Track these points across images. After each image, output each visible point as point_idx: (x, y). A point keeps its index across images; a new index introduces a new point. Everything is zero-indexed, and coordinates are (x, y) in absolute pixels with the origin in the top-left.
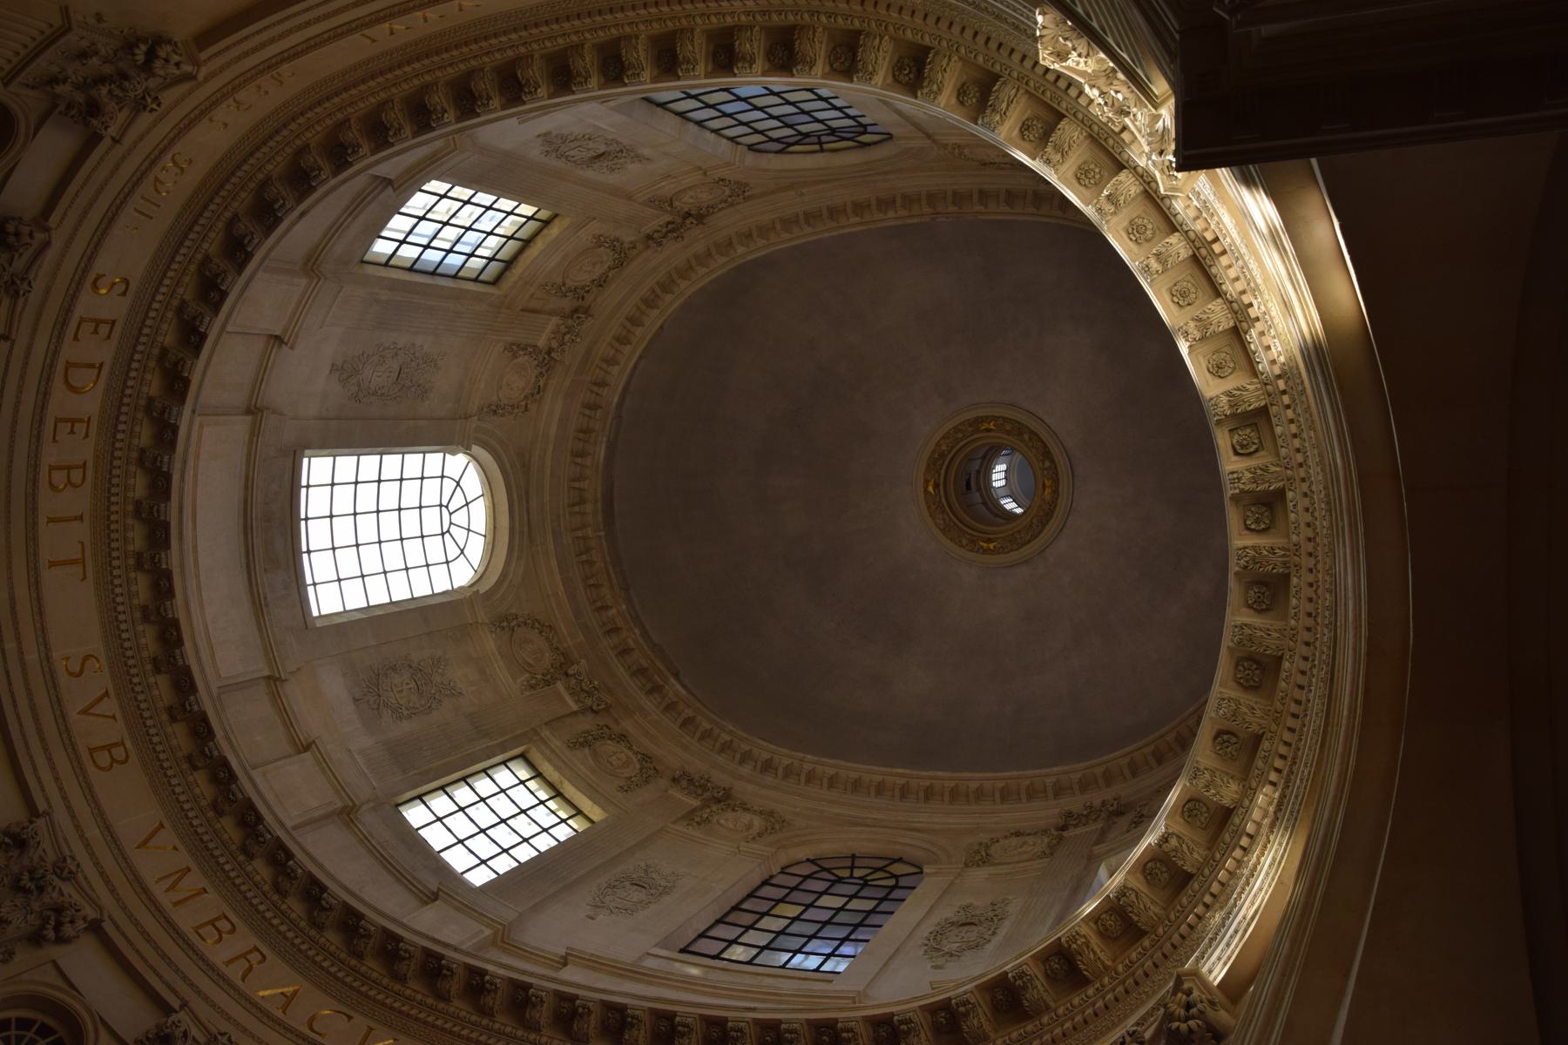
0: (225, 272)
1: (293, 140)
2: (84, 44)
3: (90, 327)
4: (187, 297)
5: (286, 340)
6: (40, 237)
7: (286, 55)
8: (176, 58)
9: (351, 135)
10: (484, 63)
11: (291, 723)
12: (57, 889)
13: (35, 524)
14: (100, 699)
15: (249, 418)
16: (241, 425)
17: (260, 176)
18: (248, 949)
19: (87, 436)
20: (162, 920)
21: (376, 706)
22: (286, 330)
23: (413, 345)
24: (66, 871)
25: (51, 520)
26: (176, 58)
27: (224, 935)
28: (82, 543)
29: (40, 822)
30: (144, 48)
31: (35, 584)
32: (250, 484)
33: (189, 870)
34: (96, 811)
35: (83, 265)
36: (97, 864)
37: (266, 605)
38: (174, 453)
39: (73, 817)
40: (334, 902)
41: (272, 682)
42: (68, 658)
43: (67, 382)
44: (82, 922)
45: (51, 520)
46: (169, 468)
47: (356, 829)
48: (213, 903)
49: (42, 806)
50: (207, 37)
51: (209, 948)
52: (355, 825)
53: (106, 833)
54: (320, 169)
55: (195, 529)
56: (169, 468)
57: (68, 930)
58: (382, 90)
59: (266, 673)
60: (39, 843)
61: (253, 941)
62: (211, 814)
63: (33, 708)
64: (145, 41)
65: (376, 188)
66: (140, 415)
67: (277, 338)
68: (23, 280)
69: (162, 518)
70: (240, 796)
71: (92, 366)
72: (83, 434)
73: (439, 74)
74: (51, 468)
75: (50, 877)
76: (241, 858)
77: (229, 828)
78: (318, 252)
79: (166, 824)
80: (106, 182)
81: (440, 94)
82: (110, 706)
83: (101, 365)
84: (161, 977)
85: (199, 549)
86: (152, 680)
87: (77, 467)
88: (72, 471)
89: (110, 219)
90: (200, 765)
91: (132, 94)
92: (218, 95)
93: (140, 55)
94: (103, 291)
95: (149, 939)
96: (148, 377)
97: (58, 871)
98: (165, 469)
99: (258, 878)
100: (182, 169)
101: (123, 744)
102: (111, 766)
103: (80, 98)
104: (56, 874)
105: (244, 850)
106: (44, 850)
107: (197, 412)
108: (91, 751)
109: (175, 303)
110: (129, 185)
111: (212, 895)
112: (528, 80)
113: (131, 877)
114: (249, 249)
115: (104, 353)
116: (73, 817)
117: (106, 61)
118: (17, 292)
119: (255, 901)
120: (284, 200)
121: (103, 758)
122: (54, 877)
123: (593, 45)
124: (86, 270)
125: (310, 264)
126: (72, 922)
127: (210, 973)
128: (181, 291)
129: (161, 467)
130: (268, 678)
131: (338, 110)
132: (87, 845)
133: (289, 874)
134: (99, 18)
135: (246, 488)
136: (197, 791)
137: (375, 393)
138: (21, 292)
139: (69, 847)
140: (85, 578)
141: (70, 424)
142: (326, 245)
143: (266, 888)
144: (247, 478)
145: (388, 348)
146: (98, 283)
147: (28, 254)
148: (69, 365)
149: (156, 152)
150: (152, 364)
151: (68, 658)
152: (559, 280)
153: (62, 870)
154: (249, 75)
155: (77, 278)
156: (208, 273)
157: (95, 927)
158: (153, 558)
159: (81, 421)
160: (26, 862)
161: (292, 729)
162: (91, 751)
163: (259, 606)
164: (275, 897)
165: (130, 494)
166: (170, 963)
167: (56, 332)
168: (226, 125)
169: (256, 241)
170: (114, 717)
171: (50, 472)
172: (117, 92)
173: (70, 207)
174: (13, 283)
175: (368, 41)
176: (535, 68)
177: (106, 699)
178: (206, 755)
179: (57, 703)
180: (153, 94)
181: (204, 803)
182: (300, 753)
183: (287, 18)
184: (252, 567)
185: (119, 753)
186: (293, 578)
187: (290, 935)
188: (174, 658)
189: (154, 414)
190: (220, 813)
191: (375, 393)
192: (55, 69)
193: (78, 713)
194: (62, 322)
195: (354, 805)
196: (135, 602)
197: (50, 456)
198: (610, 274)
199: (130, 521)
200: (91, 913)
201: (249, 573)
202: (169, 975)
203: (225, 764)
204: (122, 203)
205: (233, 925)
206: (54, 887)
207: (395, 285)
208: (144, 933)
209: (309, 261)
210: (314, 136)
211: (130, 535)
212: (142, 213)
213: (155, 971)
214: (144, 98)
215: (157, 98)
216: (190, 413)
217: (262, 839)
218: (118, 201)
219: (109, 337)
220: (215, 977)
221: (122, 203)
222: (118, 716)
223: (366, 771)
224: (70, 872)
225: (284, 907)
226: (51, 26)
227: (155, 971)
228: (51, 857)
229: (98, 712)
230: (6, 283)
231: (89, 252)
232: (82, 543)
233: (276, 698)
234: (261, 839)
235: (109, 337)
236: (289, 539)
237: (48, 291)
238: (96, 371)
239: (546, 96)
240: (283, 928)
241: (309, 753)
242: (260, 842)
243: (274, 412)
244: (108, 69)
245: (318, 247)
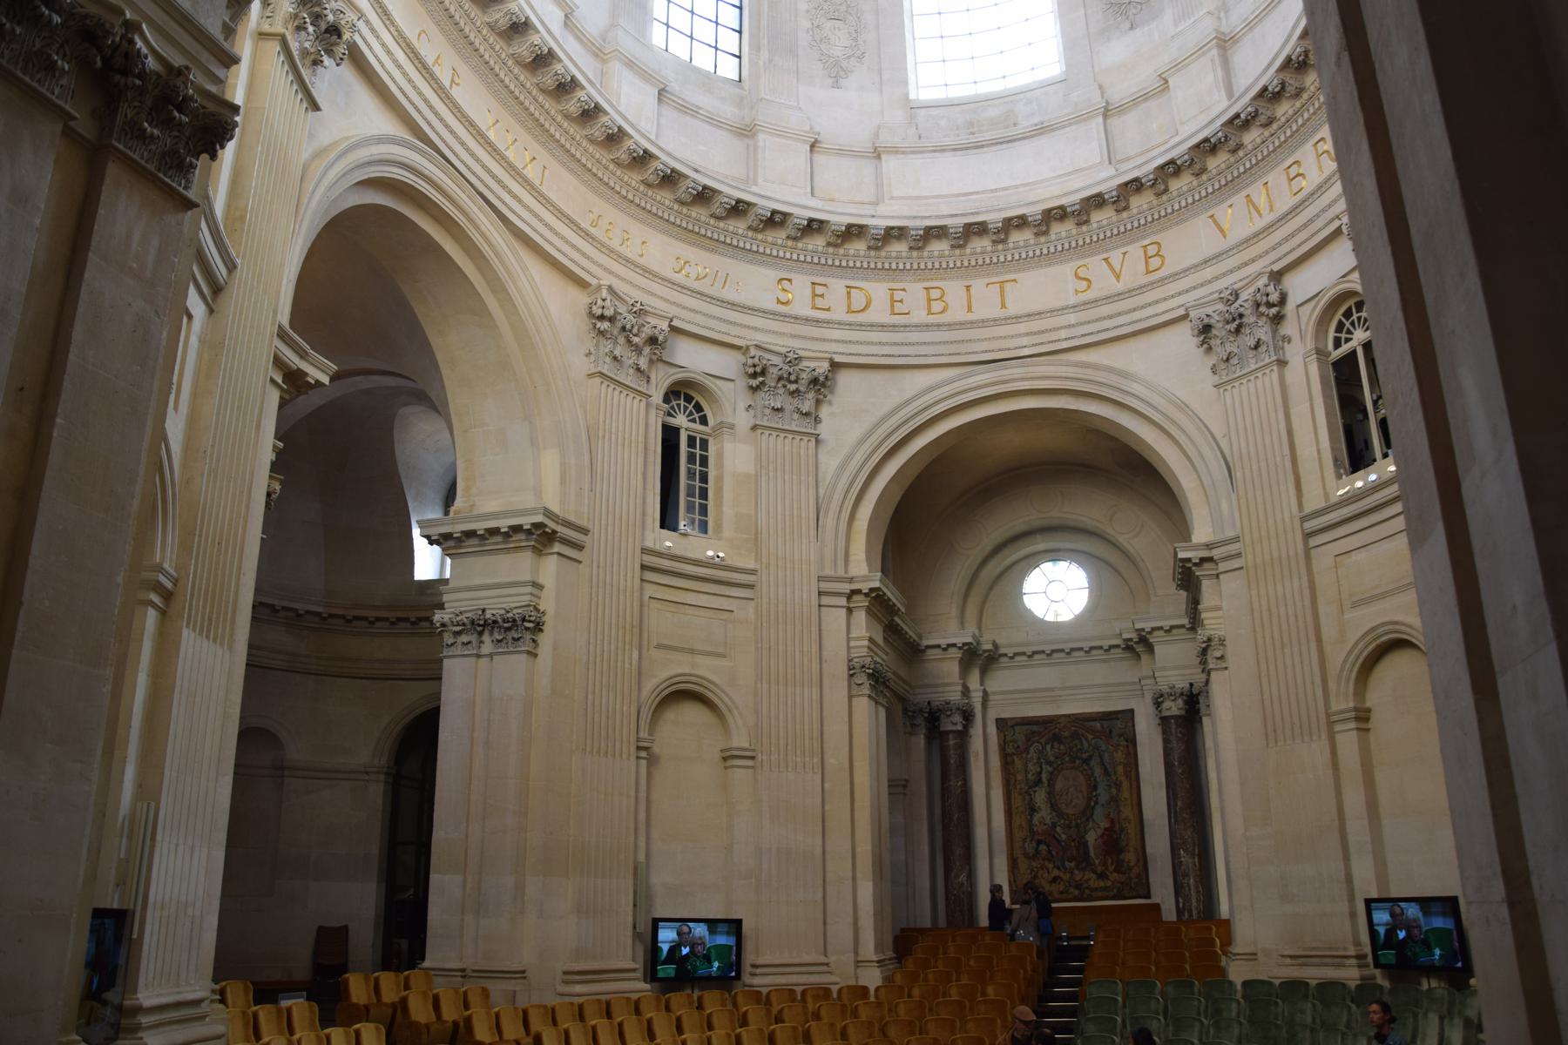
0: (756, 216)
1: (641, 192)
2: (608, 360)
3: (818, 300)
4: (784, 236)
5: (813, 140)
6: (753, 352)
7: (575, 228)
8: (600, 302)
9: (622, 156)
10: (532, 85)
11: (1145, 94)
12: (1242, 304)
13: (971, 322)
14: (1109, 264)
15: (884, 157)
16: (890, 163)
17: (676, 207)
18: (1314, 152)
19: (904, 290)
20: (1280, 224)
21: (1139, 7)
22: (805, 142)
23: (808, 11)
24: (1230, 297)
25: (970, 309)
26: (600, 302)
27: (1301, 172)
28: (988, 284)
29: (1192, 314)
30: (599, 324)
31: (1017, 319)
32: (939, 148)
33: (1248, 196)
34: (1192, 271)
35: (771, 316)
36: (1231, 271)
37: (1042, 124)
38: (907, 227)
39: (1194, 288)
40: (1275, 81)
41: (1109, 113)
42: (1076, 290)
43: (859, 312)
44: (1269, 288)
45: (970, 309)
46: (921, 229)
47: (1240, 34)
48: (1276, 177)
49: (1181, 312)
50: (582, 284)
51: (1307, 185)
52: (1236, 34)
53: (1209, 263)
54: (656, 170)
55: (977, 193)
56: (921, 229)
57: (1274, 297)
58: (581, 146)
59: (1100, 119)
60: (1208, 316)
61: (1309, 146)
62: (1204, 177)
63: (1111, 317)
64: (595, 325)
65: (670, 99)
66: (883, 254)
67: (812, 146)
68: (786, 356)
69: (961, 230)
70: (1186, 157)
71: (849, 293)
72: (904, 293)
73: (553, 112)
74: (930, 313)
75: (1232, 309)
76: (1241, 153)
77: (1215, 163)
78: (734, 129)
79: (1210, 213)
80: (705, 315)
81: (568, 106)
82: (1115, 256)
83: (847, 287)
84: (1320, 230)
85: (993, 187)
86: (1095, 225)
87: (928, 294)
88: (931, 298)
89: (732, 305)
90: (1163, 187)
91: (634, 321)
92: (620, 260)
93: (605, 325)
94: (790, 295)
95: (1292, 235)
96: (851, 252)
97: (1230, 302)
98: (922, 232)
99: (1258, 140)
100: (685, 263)
101: (1146, 246)
102: (1160, 256)
103: (647, 350)
104: (1231, 304)
105: (1234, 151)
106: (1214, 312)
107: (874, 214)
108: (1148, 272)
109: (790, 243)
110: (704, 298)
111: (1270, 178)
112: (531, 52)
113: (1245, 245)
114: (734, 203)
115: (837, 286)
116: (1194, 288)
117: (616, 343)
118: (796, 359)
119: (1277, 144)
120: (688, 188)
121: (1155, 262)
122: (1232, 306)
123: (485, 13)
124: (774, 314)
125: (746, 133)
126: (1268, 295)
127: (1324, 189)
128: (780, 241)
129: (921, 236)
130: (1105, 116)
131: (607, 169)
132: (1217, 278)
133: (1252, 117)
134: (590, 354)
135: (943, 151)
136: (1185, 188)
137: (855, 40)
138: (796, 356)
139: (1213, 293)
140: (1014, 280)
141: (895, 304)
142: (725, 124)
143: (1266, 134)
144: (934, 151)
145: (813, 36)
146: (784, 301)
147: (767, 356)
148: (850, 311)
149: (675, 287)
150: (841, 251)
151: (1076, 290)
153: (1229, 300)
154: (598, 246)
156: (761, 226)
157: (1277, 276)
158: (995, 233)
159: (892, 295)
160: (1221, 325)
161: (1150, 94)
162: (1148, 272)
163: (1042, 130)
164: (1275, 126)
165: (947, 253)
166: (1311, 221)
168: (643, 243)
169: (726, 200)
170: (1125, 253)
171: (933, 314)
172: (635, 331)
173: (729, 334)
174: (790, 362)
175: (547, 172)
176: (520, 50)
177: (1109, 260)
178: (1153, 184)
179: (1109, 299)
180: (631, 307)
181: (1195, 183)
182: (1168, 87)
183: (547, 240)
184: (1010, 138)
185: (1152, 250)
186: (1022, 95)
187: (1306, 115)
188: (1074, 212)
189: (880, 245)
190: (1203, 170)
191: (855, 40)
192: (631, 371)
193: (1118, 282)
194: (818, 322)
195: (1216, 37)
196: (1032, 242)
197: (919, 316)
199: (968, 251)
200: (1264, 280)
201: (1015, 140)
202: (1319, 223)
203: (1162, 167)
204: (718, 300)
205: (1294, 163)
206: (1241, 306)
207: (756, 48)
208: (1286, 239)
209: (743, 135)
210: (632, 179)
211: (979, 250)
212: (725, 282)
213: (1315, 234)
214: (635, 312)
215: (632, 305)
216: (874, 219)
217: (1223, 140)
218: (718, 303)
219: (825, 285)
220: (1327, 186)
221: (718, 300)
222: (1124, 250)
223: (1193, 19)
224: (1231, 294)
225: (1283, 120)
226: (602, 382)
227: (1315, 234)
228: (1221, 307)
229: (1119, 266)
230: (790, 367)
231: (760, 314)
232: (988, 284)
233: (1122, 109)
234: (1223, 140)
235: (825, 285)
236: (989, 103)
237: (793, 336)
238: (853, 290)
239: (539, 35)
240: (1300, 121)
241: (1169, 80)
242: (1226, 140)
243: (877, 135)
244: (622, 340)
245: (731, 131)
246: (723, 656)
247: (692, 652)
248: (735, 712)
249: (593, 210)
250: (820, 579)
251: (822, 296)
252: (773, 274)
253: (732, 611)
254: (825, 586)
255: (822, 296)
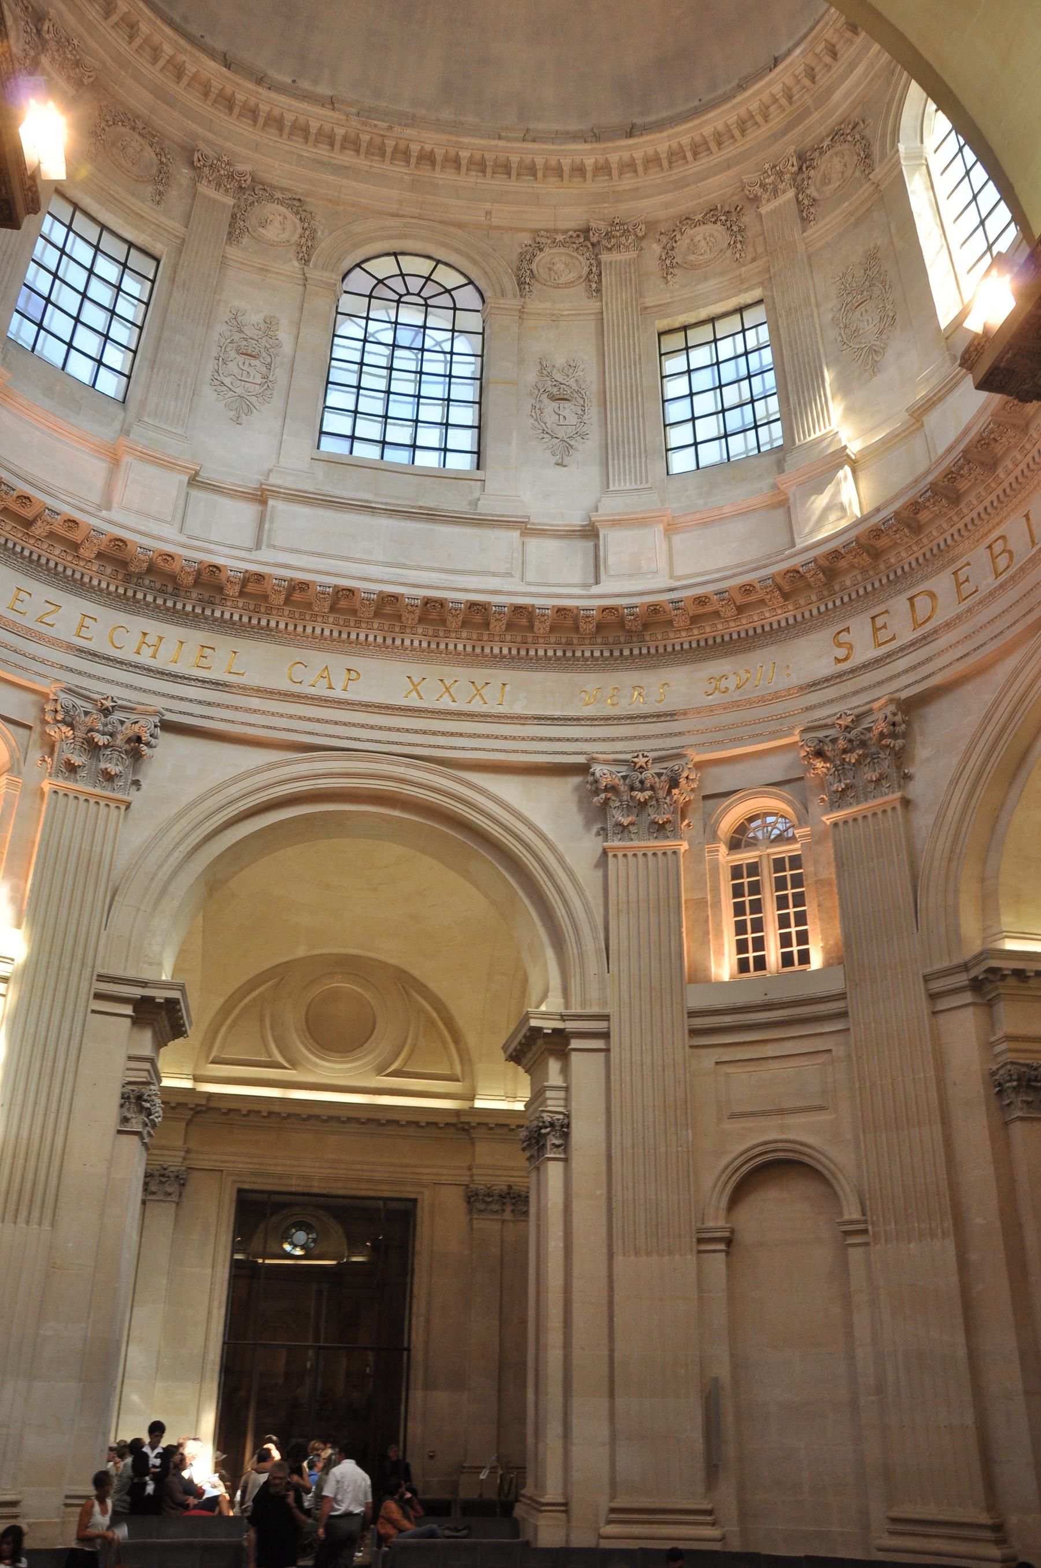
19: (968, 564)
35: (825, 685)
71: (912, 605)
124: (840, 675)
152: (729, 252)
155: (838, 680)
167: (888, 660)
198: (700, 217)
237: (856, 693)
246: (822, 1108)
247: (781, 1112)
248: (840, 1176)
249: (587, 688)
250: (927, 979)
251: (885, 626)
252: (826, 634)
253: (830, 1050)
254: (937, 986)
255: (885, 626)
